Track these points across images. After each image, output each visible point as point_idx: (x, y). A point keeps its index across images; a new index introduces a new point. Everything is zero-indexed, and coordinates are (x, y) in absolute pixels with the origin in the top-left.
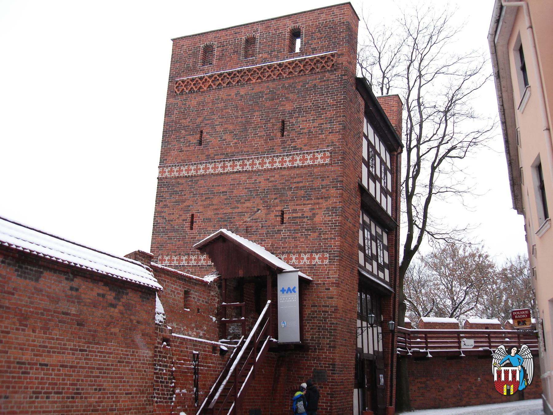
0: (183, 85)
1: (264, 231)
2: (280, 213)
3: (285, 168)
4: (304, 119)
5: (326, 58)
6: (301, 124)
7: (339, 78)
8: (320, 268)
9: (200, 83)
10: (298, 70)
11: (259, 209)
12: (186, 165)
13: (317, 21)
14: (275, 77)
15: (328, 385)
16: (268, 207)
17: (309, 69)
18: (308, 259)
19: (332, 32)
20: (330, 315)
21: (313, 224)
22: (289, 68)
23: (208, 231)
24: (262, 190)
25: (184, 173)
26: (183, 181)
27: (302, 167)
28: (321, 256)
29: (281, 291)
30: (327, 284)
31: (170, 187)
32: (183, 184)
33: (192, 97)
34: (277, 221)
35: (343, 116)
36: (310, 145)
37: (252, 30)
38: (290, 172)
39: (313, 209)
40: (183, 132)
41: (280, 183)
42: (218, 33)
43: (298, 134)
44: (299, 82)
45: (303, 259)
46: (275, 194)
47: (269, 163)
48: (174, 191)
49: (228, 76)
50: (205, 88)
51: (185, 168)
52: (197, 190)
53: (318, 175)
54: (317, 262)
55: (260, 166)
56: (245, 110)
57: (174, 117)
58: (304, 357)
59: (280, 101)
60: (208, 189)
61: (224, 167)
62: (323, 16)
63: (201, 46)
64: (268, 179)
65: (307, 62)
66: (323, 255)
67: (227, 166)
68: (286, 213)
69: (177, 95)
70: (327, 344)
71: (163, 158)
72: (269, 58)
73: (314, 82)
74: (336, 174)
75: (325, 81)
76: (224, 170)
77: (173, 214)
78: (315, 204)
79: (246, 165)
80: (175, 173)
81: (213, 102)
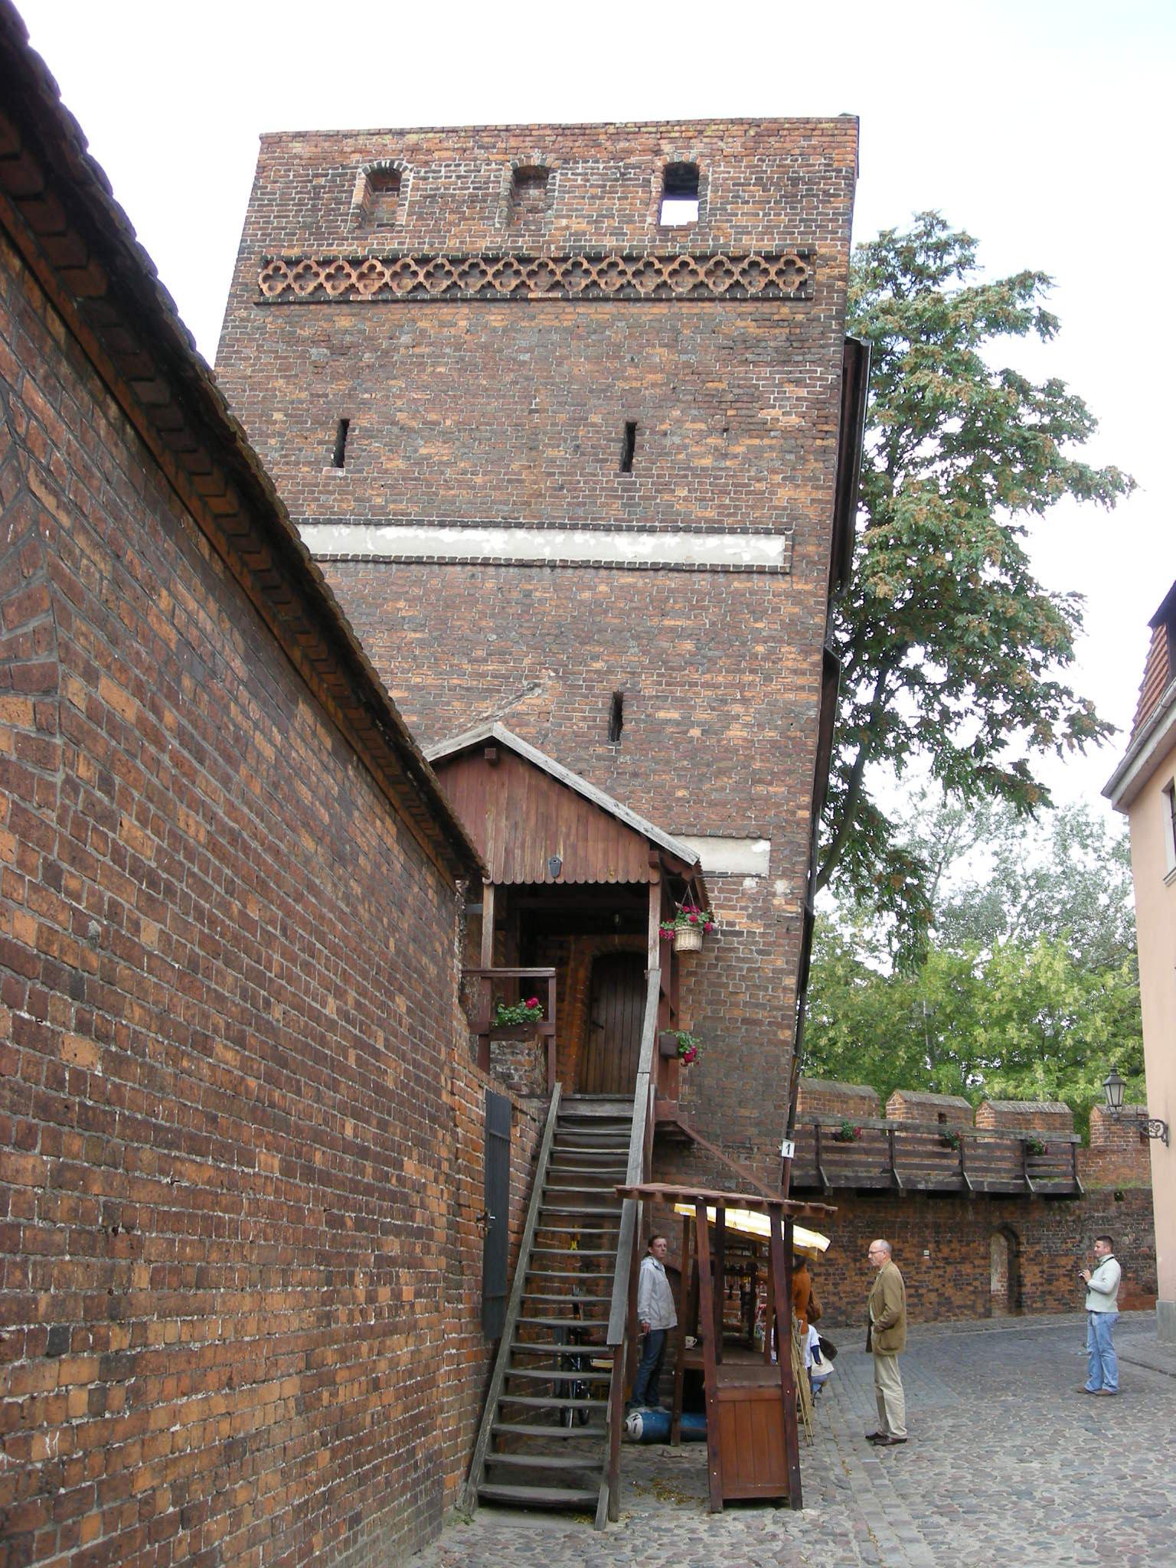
5: (783, 260)
36: (719, 507)
72: (591, 234)
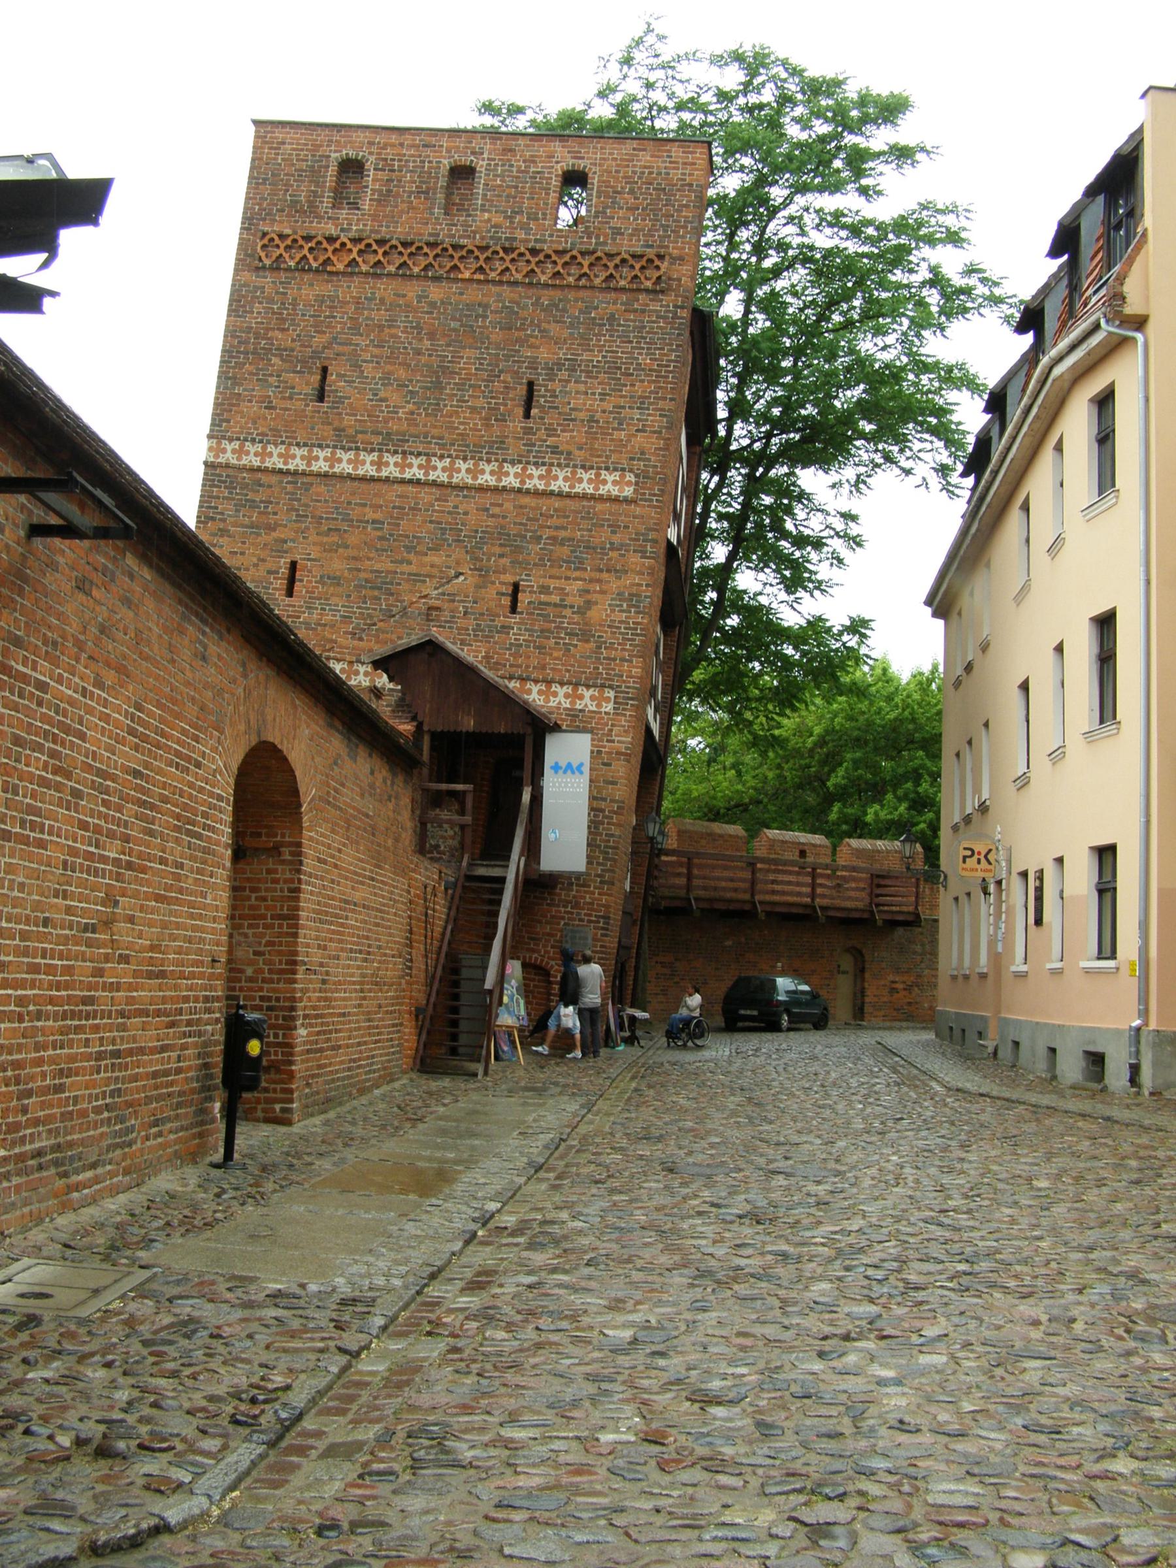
0: (282, 246)
1: (471, 623)
3: (528, 492)
4: (582, 387)
10: (574, 270)
12: (283, 443)
16: (483, 574)
17: (603, 275)
22: (555, 262)
26: (274, 479)
27: (568, 496)
32: (270, 486)
34: (501, 606)
39: (588, 592)
40: (274, 360)
44: (576, 300)
45: (555, 694)
47: (492, 473)
49: (400, 249)
52: (307, 505)
57: (252, 321)
61: (379, 464)
62: (645, 158)
63: (333, 155)
64: (487, 510)
65: (599, 259)
67: (387, 464)
69: (264, 268)
73: (611, 308)
75: (635, 311)
76: (379, 470)
77: (242, 553)
79: (435, 468)
80: (251, 457)
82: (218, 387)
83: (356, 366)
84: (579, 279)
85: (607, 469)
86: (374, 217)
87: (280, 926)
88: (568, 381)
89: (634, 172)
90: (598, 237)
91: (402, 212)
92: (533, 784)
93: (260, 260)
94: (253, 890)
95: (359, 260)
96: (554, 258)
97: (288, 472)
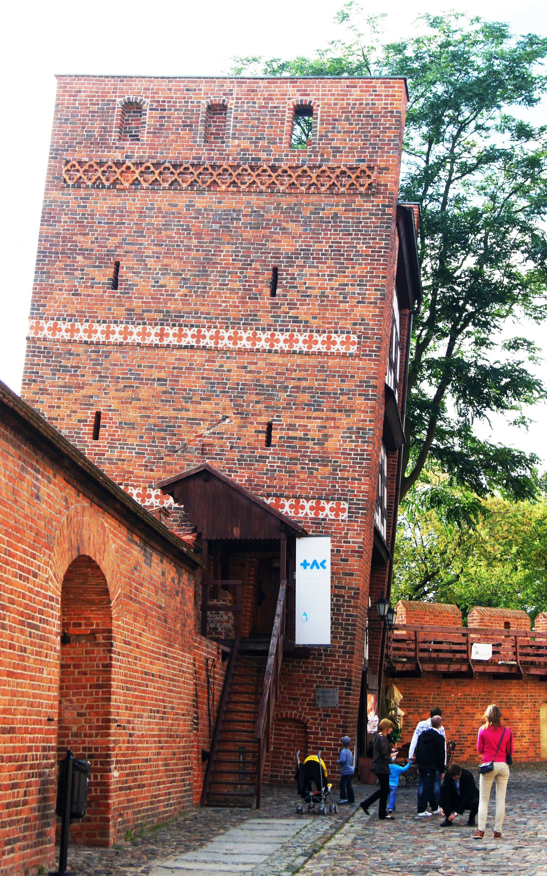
0: (82, 170)
1: (236, 455)
2: (266, 427)
3: (276, 352)
4: (314, 271)
5: (359, 170)
6: (309, 279)
7: (379, 210)
8: (333, 524)
9: (115, 172)
11: (227, 417)
12: (87, 321)
13: (343, 100)
14: (263, 188)
15: (340, 712)
17: (328, 184)
18: (312, 508)
19: (370, 124)
20: (347, 601)
21: (324, 453)
22: (290, 176)
23: (127, 444)
24: (234, 384)
25: (81, 336)
26: (81, 349)
27: (307, 354)
28: (334, 506)
29: (302, 564)
30: (344, 551)
31: (52, 357)
32: (78, 355)
33: (98, 195)
35: (383, 277)
36: (323, 318)
37: (220, 90)
38: (286, 359)
39: (325, 427)
40: (79, 258)
41: (267, 377)
42: (151, 81)
43: (302, 296)
44: (307, 205)
46: (257, 394)
47: (248, 339)
48: (60, 366)
49: (172, 170)
50: (127, 185)
51: (84, 327)
52: (107, 369)
53: (335, 372)
54: (327, 515)
55: (231, 342)
56: (203, 238)
57: (59, 228)
58: (302, 667)
59: (271, 232)
60: (130, 370)
62: (356, 92)
64: (245, 367)
65: (323, 171)
66: (338, 505)
67: (167, 335)
68: (276, 429)
69: (68, 186)
70: (340, 647)
71: (37, 301)
73: (335, 209)
74: (365, 373)
75: (353, 210)
76: (161, 340)
77: (59, 407)
78: (327, 419)
79: (204, 337)
80: (63, 333)
81: (141, 212)
82: (36, 280)
83: (141, 260)
84: (309, 188)
85: (336, 332)
86: (152, 146)
87: (97, 693)
88: (305, 267)
89: (348, 104)
90: (322, 155)
91: (172, 141)
92: (288, 578)
93: (65, 181)
94: (76, 666)
95: (141, 179)
96: (290, 172)
97: (92, 343)
